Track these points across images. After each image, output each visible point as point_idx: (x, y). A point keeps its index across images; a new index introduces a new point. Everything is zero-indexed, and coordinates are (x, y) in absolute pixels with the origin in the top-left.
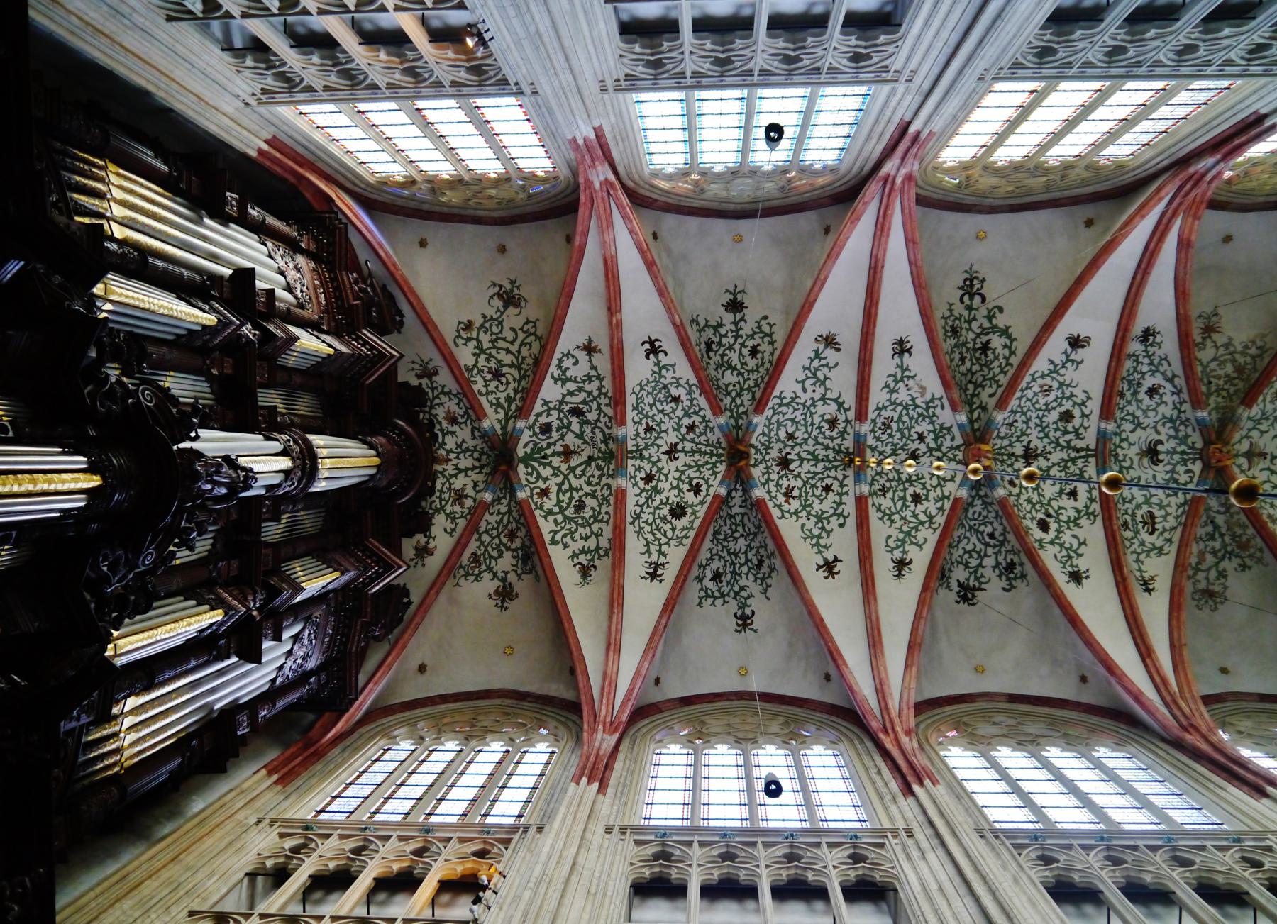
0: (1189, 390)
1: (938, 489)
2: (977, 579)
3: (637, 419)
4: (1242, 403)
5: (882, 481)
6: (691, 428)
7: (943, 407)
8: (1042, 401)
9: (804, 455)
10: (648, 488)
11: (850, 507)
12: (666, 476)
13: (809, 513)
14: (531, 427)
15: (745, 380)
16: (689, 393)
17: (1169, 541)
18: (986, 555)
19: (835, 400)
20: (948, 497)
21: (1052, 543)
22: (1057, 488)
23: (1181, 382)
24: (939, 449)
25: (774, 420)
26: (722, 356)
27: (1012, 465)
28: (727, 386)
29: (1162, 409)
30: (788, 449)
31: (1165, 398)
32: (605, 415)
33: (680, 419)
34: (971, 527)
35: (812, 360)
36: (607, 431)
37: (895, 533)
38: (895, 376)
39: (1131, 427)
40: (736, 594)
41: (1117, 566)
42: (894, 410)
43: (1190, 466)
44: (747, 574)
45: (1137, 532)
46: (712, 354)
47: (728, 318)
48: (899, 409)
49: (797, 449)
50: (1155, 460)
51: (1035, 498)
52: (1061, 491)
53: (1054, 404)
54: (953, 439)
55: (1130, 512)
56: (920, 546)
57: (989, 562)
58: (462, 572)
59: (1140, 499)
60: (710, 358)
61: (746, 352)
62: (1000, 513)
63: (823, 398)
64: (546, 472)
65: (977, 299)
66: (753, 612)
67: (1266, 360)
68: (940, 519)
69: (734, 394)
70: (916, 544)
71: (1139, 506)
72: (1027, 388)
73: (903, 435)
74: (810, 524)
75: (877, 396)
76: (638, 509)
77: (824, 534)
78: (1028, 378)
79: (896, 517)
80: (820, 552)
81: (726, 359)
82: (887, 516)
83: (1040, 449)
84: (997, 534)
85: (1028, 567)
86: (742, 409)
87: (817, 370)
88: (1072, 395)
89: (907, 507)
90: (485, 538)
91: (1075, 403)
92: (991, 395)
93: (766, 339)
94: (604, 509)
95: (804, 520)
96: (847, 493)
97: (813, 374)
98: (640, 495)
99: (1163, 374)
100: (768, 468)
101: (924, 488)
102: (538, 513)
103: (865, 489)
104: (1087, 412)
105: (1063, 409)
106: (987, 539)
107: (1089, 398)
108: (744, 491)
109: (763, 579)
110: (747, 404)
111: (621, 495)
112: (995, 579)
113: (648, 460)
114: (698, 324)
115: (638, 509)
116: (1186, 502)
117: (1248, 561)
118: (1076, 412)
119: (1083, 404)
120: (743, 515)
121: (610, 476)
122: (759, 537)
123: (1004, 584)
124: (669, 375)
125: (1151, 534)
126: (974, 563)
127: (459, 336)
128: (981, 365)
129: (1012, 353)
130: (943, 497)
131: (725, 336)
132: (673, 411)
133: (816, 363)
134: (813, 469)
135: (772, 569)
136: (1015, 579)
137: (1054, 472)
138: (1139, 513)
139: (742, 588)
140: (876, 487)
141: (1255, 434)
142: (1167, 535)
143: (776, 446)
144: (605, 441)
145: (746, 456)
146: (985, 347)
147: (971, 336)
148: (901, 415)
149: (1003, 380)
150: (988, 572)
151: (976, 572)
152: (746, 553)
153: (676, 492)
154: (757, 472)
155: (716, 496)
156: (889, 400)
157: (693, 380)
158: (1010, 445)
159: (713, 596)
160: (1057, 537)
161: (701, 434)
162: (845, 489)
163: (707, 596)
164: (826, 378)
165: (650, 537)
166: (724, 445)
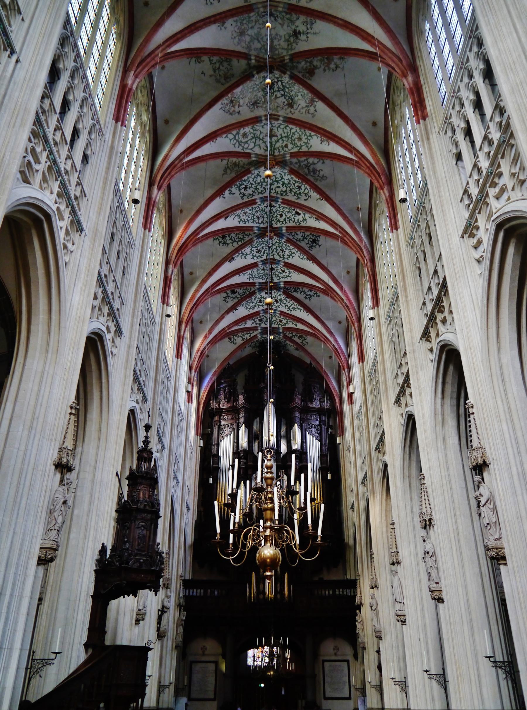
3: (257, 307)
5: (279, 250)
14: (260, 325)
27: (274, 212)
39: (259, 177)
48: (253, 249)
55: (294, 182)
58: (304, 342)
60: (237, 292)
64: (274, 319)
72: (244, 221)
73: (263, 243)
76: (287, 307)
90: (294, 334)
102: (287, 326)
114: (225, 298)
115: (287, 307)
127: (233, 342)
140: (281, 253)
148: (256, 247)
158: (266, 213)
163: (316, 293)
165: (296, 307)
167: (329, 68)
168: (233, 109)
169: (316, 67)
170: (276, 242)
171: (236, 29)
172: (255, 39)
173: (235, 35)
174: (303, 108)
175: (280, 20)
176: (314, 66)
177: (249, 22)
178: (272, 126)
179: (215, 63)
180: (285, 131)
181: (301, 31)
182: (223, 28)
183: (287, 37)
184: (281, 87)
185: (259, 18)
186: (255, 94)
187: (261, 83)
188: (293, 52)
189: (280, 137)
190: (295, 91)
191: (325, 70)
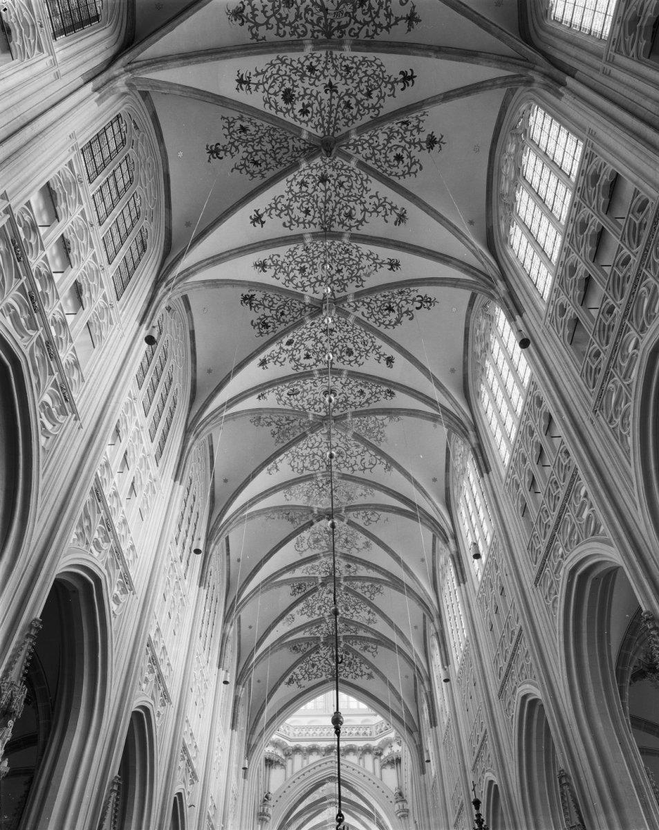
0: (361, 411)
1: (309, 283)
2: (257, 305)
3: (356, 60)
4: (354, 433)
6: (348, 105)
7: (357, 286)
8: (358, 340)
9: (328, 193)
10: (305, 68)
11: (297, 230)
12: (313, 84)
13: (291, 200)
15: (380, 151)
16: (374, 107)
17: (285, 404)
18: (271, 310)
19: (364, 219)
20: (304, 290)
21: (281, 348)
22: (311, 348)
23: (366, 407)
24: (333, 282)
25: (352, 173)
26: (398, 132)
28: (377, 136)
29: (352, 396)
30: (332, 182)
31: (358, 398)
32: (360, 29)
33: (355, 96)
34: (286, 302)
35: (390, 204)
36: (347, 30)
37: (281, 259)
38: (377, 259)
39: (343, 382)
40: (233, 144)
41: (271, 384)
42: (356, 256)
43: (323, 410)
44: (247, 151)
45: (288, 387)
46: (399, 125)
47: (424, 137)
48: (357, 259)
49: (333, 188)
50: (326, 393)
51: (304, 336)
52: (309, 350)
53: (357, 346)
54: (338, 291)
56: (274, 276)
57: (267, 312)
59: (305, 388)
61: (399, 151)
62: (296, 320)
63: (365, 210)
65: (419, 305)
66: (221, 158)
67: (374, 443)
68: (291, 287)
69: (371, 141)
70: (275, 273)
71: (302, 387)
73: (341, 260)
74: (284, 201)
75: (365, 248)
76: (288, 62)
77: (278, 212)
78: (371, 335)
79: (291, 259)
80: (267, 210)
81: (396, 134)
82: (292, 253)
83: (333, 337)
84: (283, 317)
85: (266, 338)
86: (360, 148)
87: (384, 207)
88: (361, 356)
89: (297, 265)
91: (357, 357)
92: (363, 314)
93: (406, 168)
94: (288, 29)
95: (286, 197)
96: (305, 227)
97: (381, 205)
98: (299, 62)
99: (370, 398)
100: (320, 167)
101: (309, 274)
103: (308, 241)
104: (352, 364)
105: (354, 350)
106: (281, 311)
107: (359, 365)
108: (304, 151)
109: (244, 165)
110: (364, 153)
111: (296, 45)
112: (258, 316)
113: (326, 68)
115: (288, 62)
116: (305, 409)
117: (276, 436)
118: (352, 358)
119: (357, 362)
120: (287, 148)
121: (313, 32)
122: (273, 163)
123: (256, 322)
124: (387, 91)
125: (288, 394)
126: (266, 303)
128: (380, 307)
129: (386, 326)
130: (304, 287)
131: (412, 134)
132: (361, 91)
133: (388, 207)
134: (319, 200)
135: (252, 174)
136: (259, 328)
137: (319, 345)
138: (298, 387)
139: (237, 148)
140: (309, 245)
141: (339, 436)
142: (288, 401)
143: (335, 174)
144: (339, 27)
145: (329, 153)
146: (390, 309)
147: (398, 301)
148: (353, 260)
149: (371, 322)
150: (261, 311)
151: (261, 304)
152: (261, 150)
153: (302, 93)
154: (318, 161)
155: (300, 130)
156: (362, 254)
157: (383, 112)
159: (230, 127)
160: (284, 350)
161: (344, 114)
162: (307, 225)
163: (229, 123)
164: (378, 212)
166: (336, 135)
170: (319, 256)
175: (323, 529)
180: (313, 441)
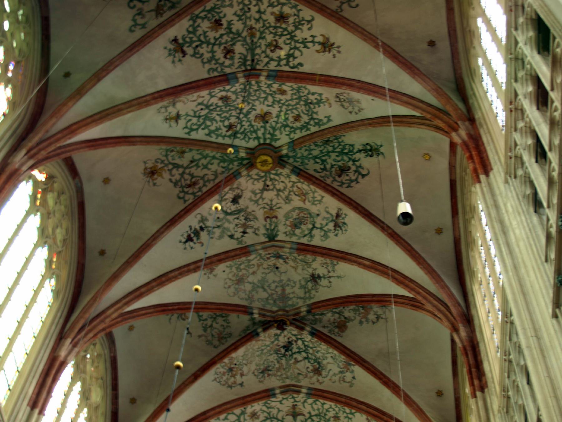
167: (367, 320)
168: (232, 379)
169: (348, 319)
171: (230, 276)
172: (258, 287)
173: (229, 283)
174: (335, 375)
176: (345, 318)
177: (248, 266)
178: (295, 401)
179: (206, 319)
181: (321, 275)
182: (211, 276)
183: (303, 283)
184: (302, 347)
185: (262, 261)
186: (264, 357)
187: (273, 342)
188: (312, 301)
189: (308, 416)
190: (323, 351)
191: (361, 323)
